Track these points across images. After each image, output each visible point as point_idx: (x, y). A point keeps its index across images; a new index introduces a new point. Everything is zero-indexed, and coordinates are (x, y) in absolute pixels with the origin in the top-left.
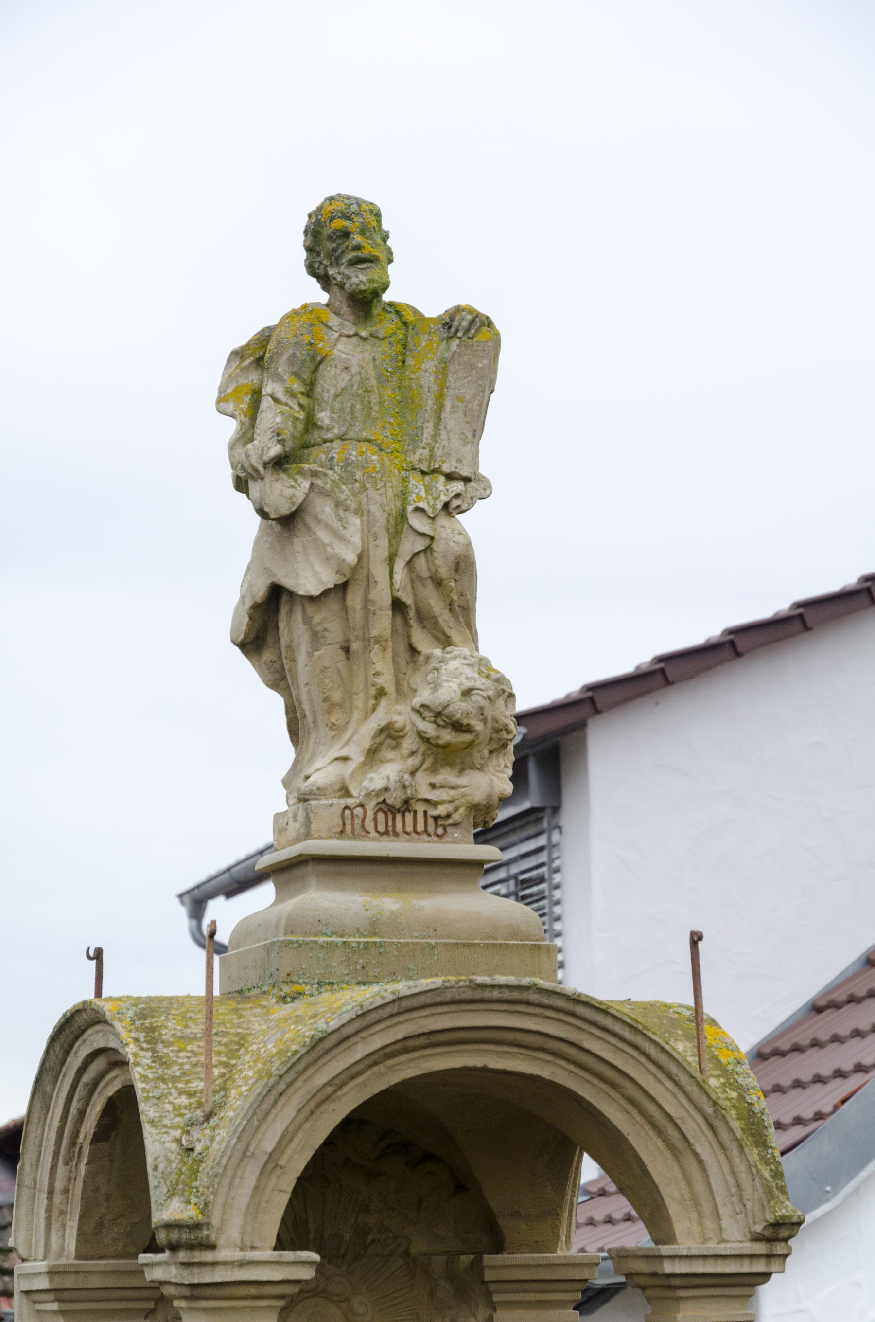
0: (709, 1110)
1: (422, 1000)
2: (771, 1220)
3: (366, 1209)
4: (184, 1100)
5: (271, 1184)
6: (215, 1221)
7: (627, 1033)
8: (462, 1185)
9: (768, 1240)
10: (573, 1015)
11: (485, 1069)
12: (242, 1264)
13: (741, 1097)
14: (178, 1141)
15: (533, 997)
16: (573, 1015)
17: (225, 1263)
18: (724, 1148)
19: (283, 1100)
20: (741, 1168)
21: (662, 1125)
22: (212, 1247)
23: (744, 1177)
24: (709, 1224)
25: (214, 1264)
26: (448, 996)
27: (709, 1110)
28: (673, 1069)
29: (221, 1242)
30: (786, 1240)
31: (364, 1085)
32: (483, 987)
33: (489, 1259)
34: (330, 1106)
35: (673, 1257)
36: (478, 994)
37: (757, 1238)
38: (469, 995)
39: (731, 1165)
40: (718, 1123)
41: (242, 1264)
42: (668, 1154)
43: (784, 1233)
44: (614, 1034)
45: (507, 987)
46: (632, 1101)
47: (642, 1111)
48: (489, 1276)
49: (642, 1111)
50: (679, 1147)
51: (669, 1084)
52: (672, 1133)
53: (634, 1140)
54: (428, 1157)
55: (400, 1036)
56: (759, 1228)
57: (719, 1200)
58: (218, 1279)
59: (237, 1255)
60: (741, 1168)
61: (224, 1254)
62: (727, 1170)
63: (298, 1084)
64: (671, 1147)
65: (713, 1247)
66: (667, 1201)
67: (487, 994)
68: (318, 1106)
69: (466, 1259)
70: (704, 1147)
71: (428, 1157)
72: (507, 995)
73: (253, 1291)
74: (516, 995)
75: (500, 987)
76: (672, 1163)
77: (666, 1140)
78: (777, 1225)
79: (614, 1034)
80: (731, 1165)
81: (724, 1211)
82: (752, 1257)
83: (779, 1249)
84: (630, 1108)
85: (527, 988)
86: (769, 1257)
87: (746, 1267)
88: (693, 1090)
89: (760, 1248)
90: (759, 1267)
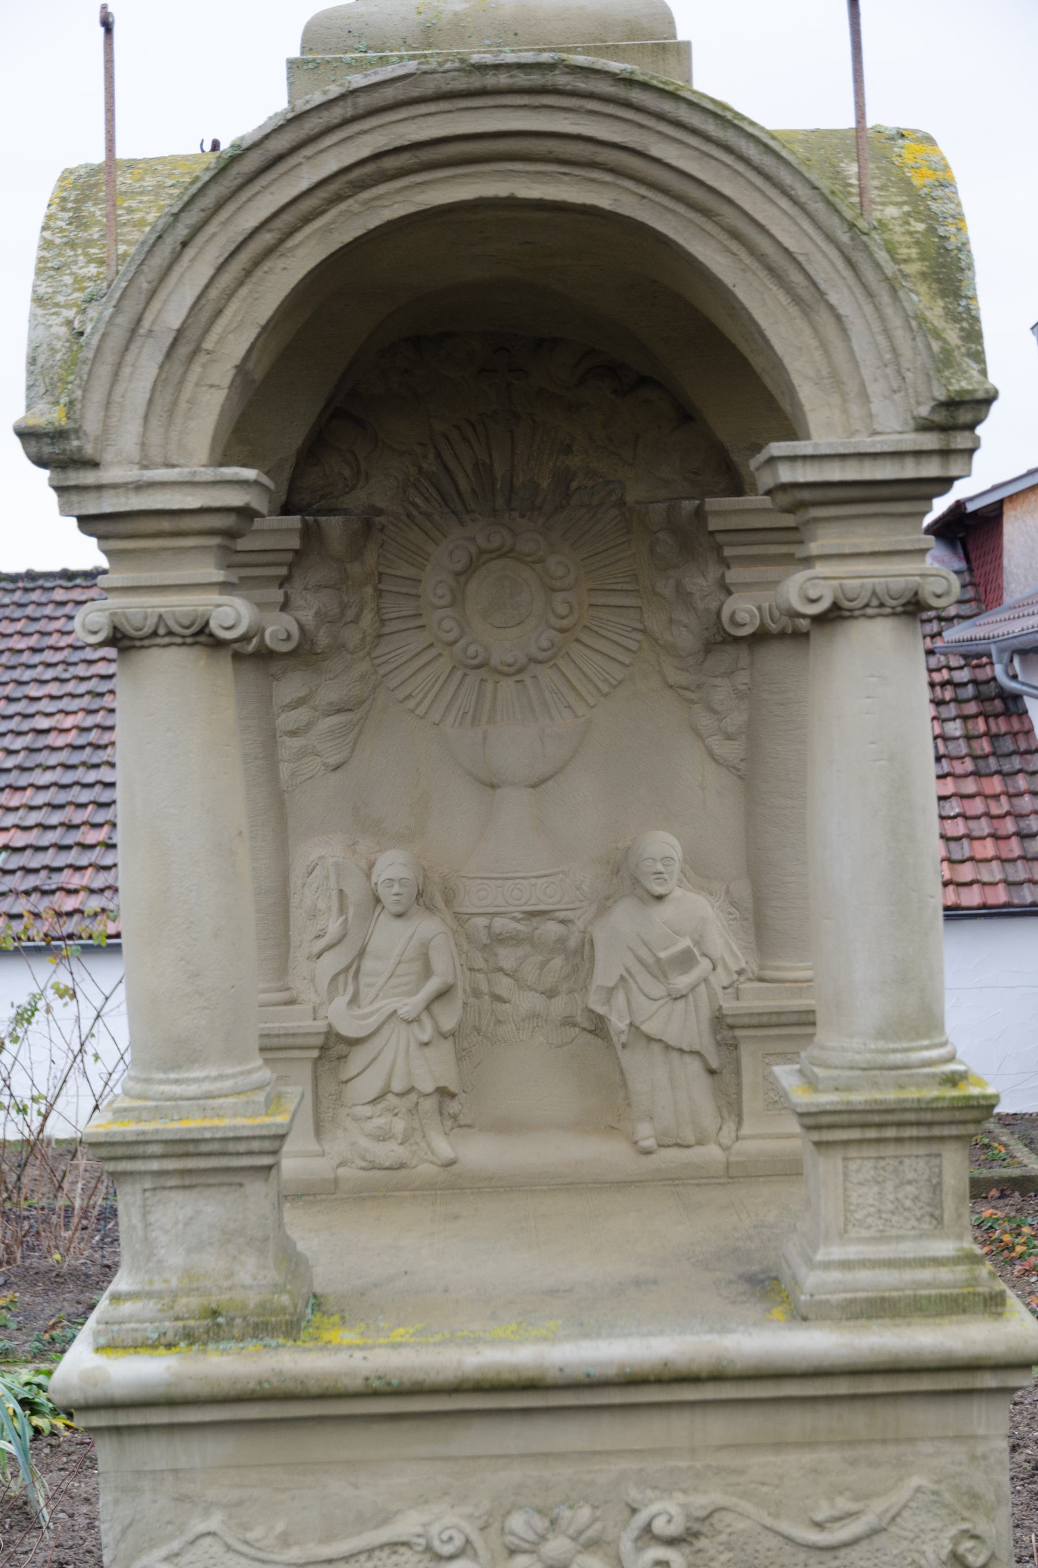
0: (845, 238)
1: (390, 94)
2: (941, 395)
3: (568, 450)
4: (92, 269)
5: (193, 376)
6: (91, 424)
7: (711, 127)
8: (686, 416)
9: (943, 429)
10: (628, 105)
11: (512, 203)
12: (140, 487)
13: (932, 230)
14: (69, 323)
15: (562, 80)
16: (628, 105)
17: (115, 486)
18: (870, 294)
19: (190, 252)
20: (896, 322)
21: (779, 267)
22: (94, 464)
23: (900, 335)
24: (855, 410)
25: (99, 488)
26: (430, 86)
27: (845, 238)
28: (786, 178)
29: (108, 456)
30: (971, 427)
31: (327, 230)
32: (482, 68)
33: (712, 503)
34: (274, 263)
35: (793, 459)
36: (476, 82)
37: (925, 426)
38: (462, 83)
39: (882, 318)
40: (858, 257)
41: (140, 487)
42: (794, 311)
43: (965, 416)
44: (695, 132)
45: (520, 66)
46: (735, 235)
47: (752, 250)
48: (713, 524)
49: (752, 250)
50: (809, 299)
51: (784, 203)
52: (796, 277)
53: (744, 294)
54: (644, 381)
55: (366, 152)
56: (924, 411)
57: (867, 373)
58: (107, 509)
59: (133, 474)
60: (896, 322)
61: (108, 475)
62: (876, 327)
63: (212, 228)
64: (797, 300)
65: (866, 443)
66: (796, 380)
67: (490, 80)
68: (257, 262)
69: (688, 506)
70: (842, 296)
71: (644, 381)
72: (522, 79)
73: (166, 525)
74: (536, 79)
75: (509, 67)
76: (800, 323)
77: (788, 289)
78: (952, 404)
79: (695, 132)
80: (882, 318)
81: (875, 390)
82: (918, 454)
83: (960, 441)
84: (734, 246)
85: (551, 67)
86: (945, 453)
87: (909, 470)
88: (818, 207)
89: (930, 441)
90: (931, 469)
